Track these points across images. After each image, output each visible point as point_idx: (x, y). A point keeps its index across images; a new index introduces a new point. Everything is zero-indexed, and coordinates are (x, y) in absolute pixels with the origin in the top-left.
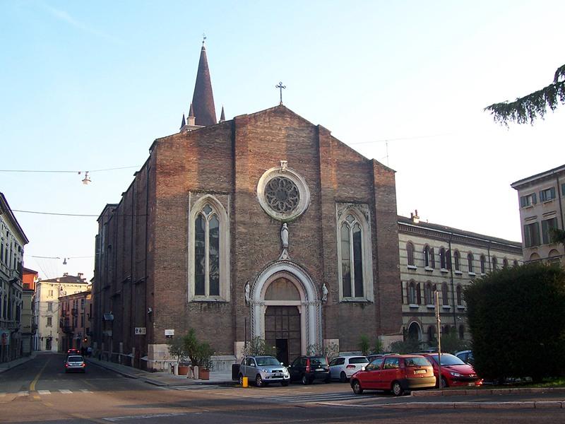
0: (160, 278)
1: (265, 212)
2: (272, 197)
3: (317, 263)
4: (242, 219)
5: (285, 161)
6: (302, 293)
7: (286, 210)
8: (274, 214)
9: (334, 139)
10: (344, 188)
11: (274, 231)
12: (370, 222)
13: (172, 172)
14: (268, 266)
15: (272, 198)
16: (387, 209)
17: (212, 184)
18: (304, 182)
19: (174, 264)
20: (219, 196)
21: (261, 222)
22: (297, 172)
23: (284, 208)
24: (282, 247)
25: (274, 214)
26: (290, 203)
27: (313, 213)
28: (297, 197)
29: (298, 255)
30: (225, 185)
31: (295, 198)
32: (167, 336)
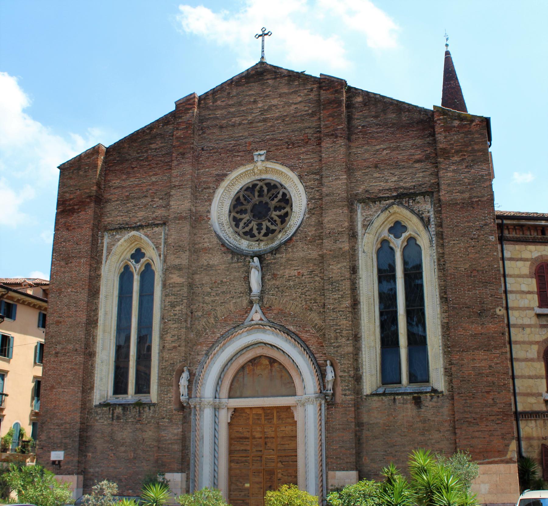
0: (49, 370)
1: (223, 245)
2: (243, 216)
3: (319, 322)
4: (177, 262)
5: (262, 152)
6: (297, 381)
7: (266, 235)
8: (244, 244)
9: (352, 92)
10: (376, 175)
11: (237, 274)
12: (432, 228)
13: (76, 207)
14: (226, 337)
15: (241, 220)
16: (467, 195)
17: (141, 214)
18: (296, 180)
19: (70, 347)
20: (148, 231)
21: (216, 263)
22: (282, 164)
23: (263, 231)
24: (251, 303)
25: (244, 244)
26: (274, 222)
27: (311, 232)
28: (287, 209)
29: (281, 312)
30: (160, 212)
31: (283, 212)
32: (54, 462)
